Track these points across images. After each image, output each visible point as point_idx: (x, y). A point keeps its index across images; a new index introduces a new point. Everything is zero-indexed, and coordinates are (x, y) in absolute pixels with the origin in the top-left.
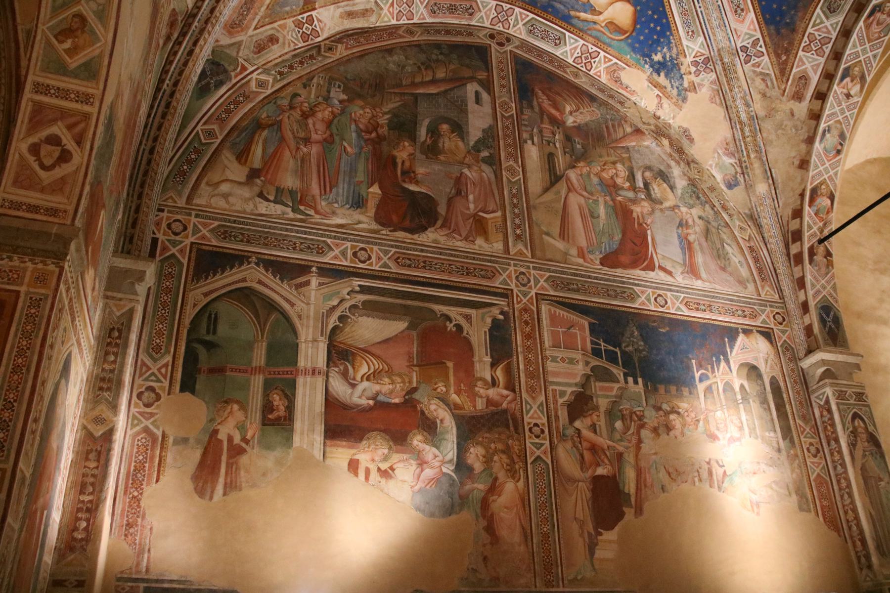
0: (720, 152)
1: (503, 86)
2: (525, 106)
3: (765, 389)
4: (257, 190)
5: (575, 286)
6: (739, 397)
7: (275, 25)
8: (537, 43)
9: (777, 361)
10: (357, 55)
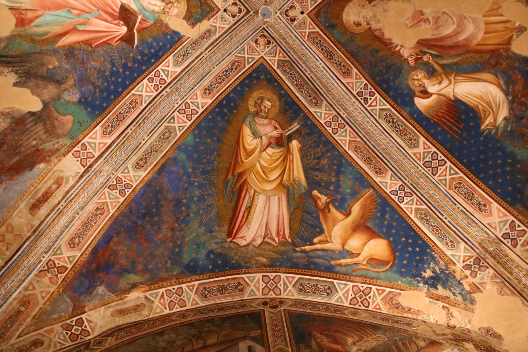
1: (278, 337)
2: (301, 348)
7: (41, 331)
8: (309, 299)
10: (126, 342)
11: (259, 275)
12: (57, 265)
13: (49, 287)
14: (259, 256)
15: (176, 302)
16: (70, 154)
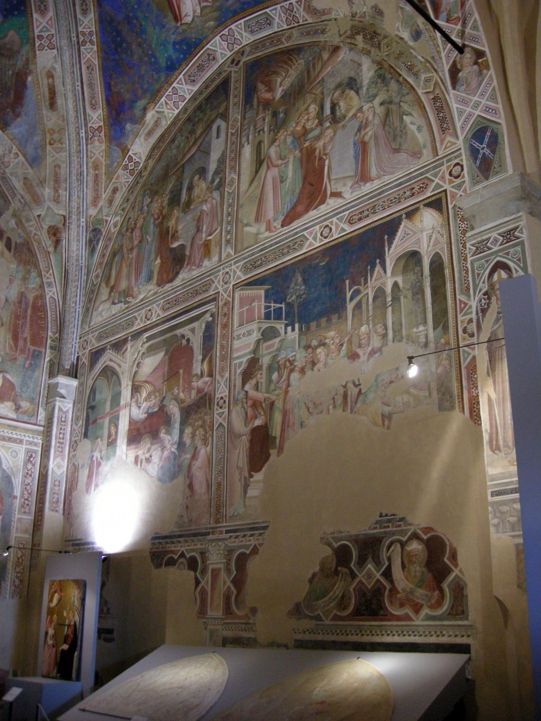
0: (401, 5)
3: (422, 274)
4: (111, 300)
5: (260, 262)
6: (389, 299)
7: (113, 181)
9: (444, 232)
11: (218, 38)
12: (96, 128)
13: (101, 147)
14: (207, 23)
15: (177, 100)
16: (37, 52)
